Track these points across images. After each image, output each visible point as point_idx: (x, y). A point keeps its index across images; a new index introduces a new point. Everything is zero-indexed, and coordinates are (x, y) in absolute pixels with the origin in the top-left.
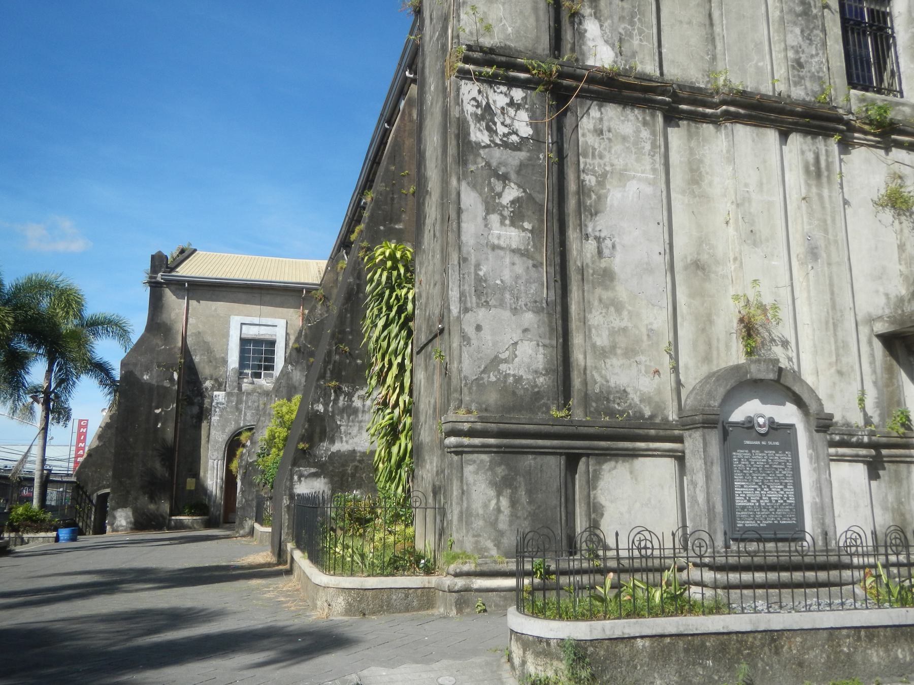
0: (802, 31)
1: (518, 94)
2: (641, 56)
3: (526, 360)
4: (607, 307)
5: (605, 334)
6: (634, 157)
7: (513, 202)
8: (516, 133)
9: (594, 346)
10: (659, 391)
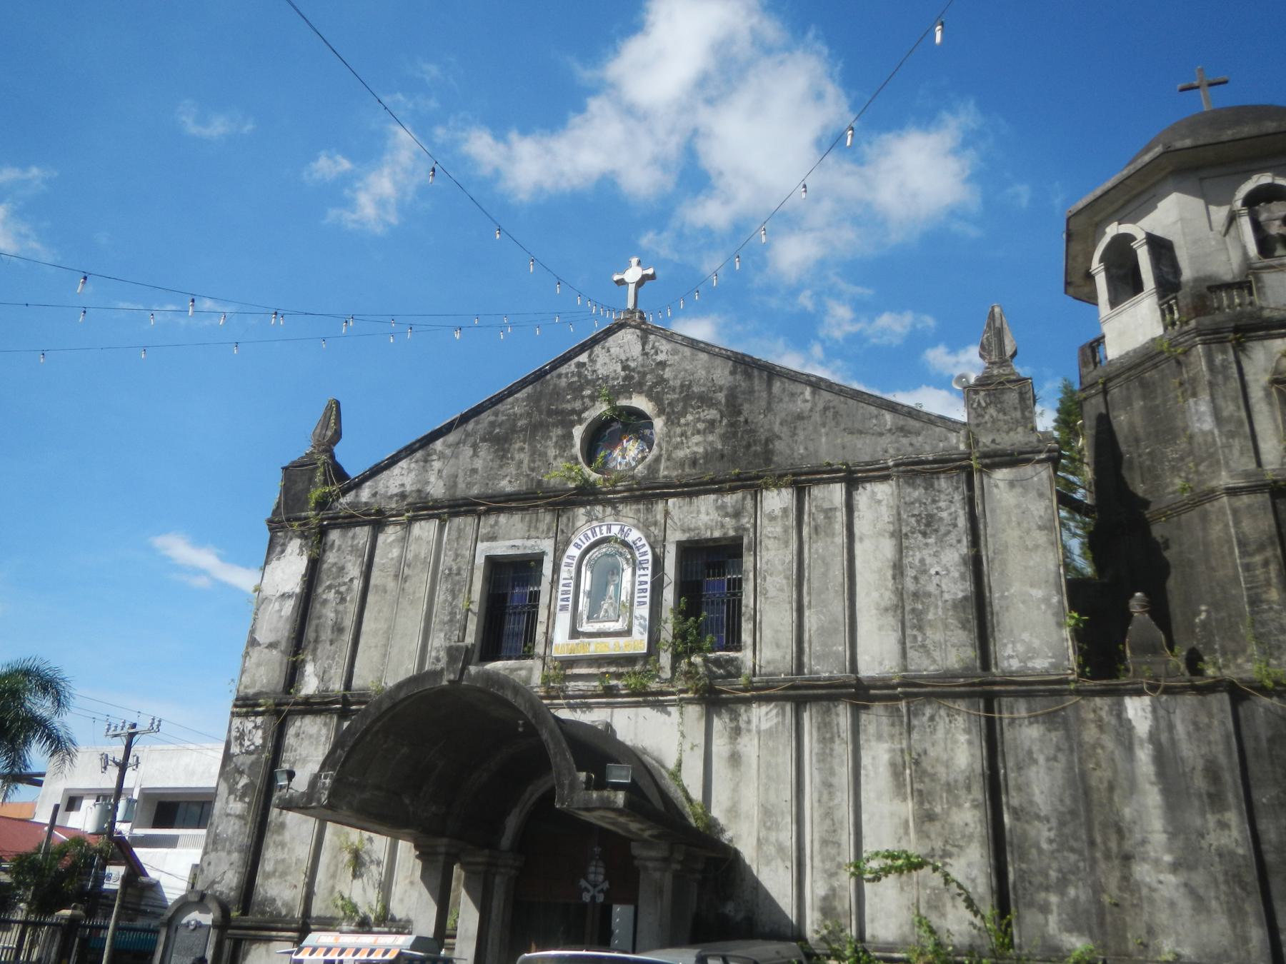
0: (445, 635)
1: (259, 720)
2: (333, 679)
3: (228, 881)
4: (277, 846)
5: (272, 863)
6: (314, 747)
7: (243, 787)
8: (253, 744)
9: (264, 872)
10: (294, 899)
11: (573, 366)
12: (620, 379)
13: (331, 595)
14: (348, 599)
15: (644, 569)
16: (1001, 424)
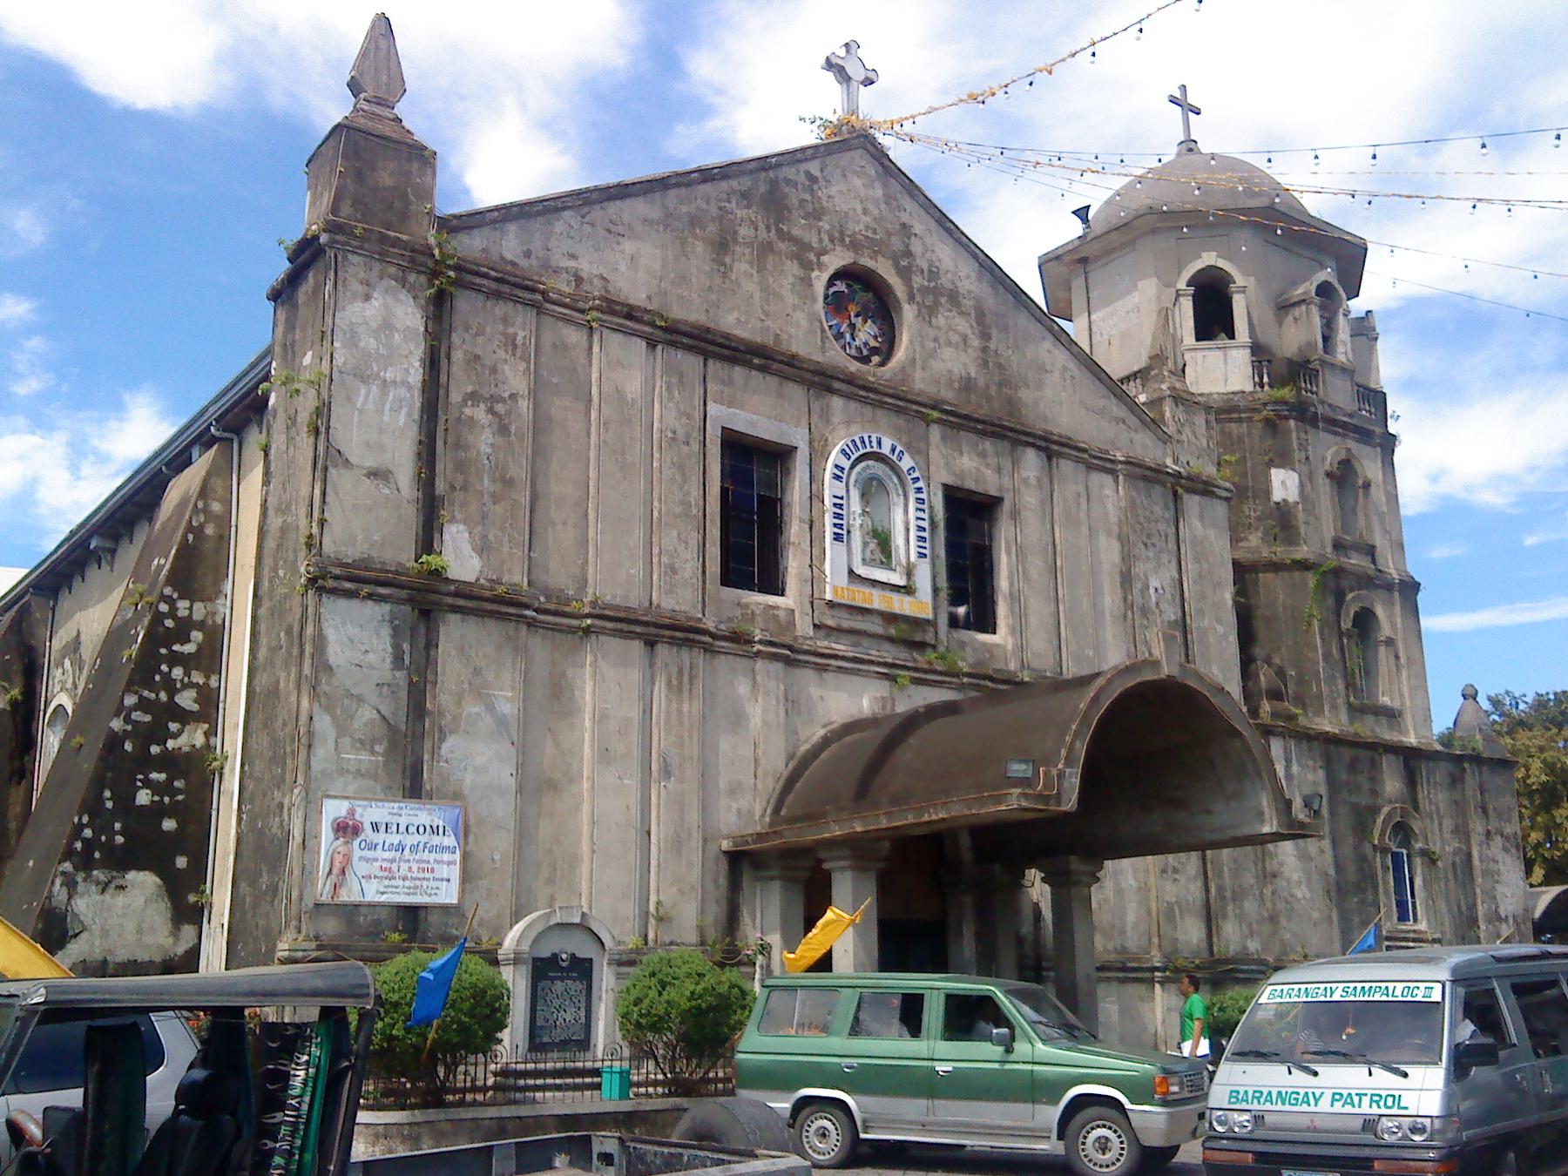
11: (802, 178)
12: (862, 227)
13: (480, 413)
14: (513, 428)
15: (920, 510)
16: (1194, 448)
